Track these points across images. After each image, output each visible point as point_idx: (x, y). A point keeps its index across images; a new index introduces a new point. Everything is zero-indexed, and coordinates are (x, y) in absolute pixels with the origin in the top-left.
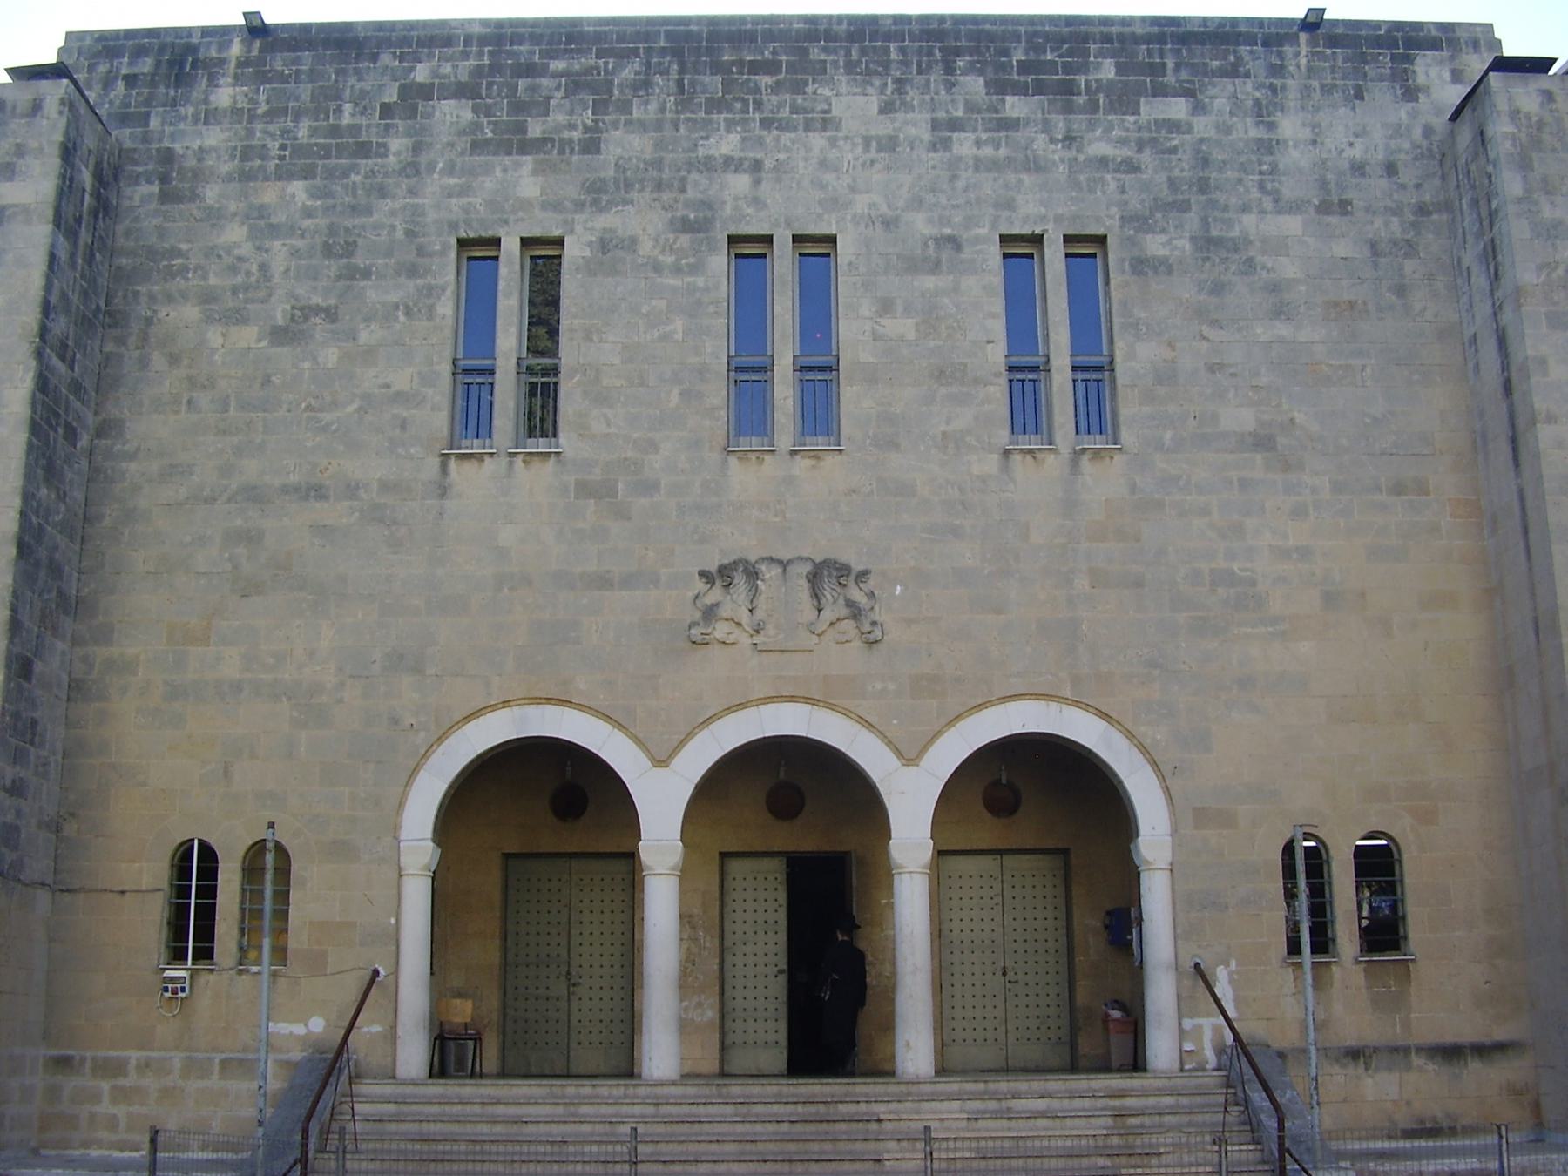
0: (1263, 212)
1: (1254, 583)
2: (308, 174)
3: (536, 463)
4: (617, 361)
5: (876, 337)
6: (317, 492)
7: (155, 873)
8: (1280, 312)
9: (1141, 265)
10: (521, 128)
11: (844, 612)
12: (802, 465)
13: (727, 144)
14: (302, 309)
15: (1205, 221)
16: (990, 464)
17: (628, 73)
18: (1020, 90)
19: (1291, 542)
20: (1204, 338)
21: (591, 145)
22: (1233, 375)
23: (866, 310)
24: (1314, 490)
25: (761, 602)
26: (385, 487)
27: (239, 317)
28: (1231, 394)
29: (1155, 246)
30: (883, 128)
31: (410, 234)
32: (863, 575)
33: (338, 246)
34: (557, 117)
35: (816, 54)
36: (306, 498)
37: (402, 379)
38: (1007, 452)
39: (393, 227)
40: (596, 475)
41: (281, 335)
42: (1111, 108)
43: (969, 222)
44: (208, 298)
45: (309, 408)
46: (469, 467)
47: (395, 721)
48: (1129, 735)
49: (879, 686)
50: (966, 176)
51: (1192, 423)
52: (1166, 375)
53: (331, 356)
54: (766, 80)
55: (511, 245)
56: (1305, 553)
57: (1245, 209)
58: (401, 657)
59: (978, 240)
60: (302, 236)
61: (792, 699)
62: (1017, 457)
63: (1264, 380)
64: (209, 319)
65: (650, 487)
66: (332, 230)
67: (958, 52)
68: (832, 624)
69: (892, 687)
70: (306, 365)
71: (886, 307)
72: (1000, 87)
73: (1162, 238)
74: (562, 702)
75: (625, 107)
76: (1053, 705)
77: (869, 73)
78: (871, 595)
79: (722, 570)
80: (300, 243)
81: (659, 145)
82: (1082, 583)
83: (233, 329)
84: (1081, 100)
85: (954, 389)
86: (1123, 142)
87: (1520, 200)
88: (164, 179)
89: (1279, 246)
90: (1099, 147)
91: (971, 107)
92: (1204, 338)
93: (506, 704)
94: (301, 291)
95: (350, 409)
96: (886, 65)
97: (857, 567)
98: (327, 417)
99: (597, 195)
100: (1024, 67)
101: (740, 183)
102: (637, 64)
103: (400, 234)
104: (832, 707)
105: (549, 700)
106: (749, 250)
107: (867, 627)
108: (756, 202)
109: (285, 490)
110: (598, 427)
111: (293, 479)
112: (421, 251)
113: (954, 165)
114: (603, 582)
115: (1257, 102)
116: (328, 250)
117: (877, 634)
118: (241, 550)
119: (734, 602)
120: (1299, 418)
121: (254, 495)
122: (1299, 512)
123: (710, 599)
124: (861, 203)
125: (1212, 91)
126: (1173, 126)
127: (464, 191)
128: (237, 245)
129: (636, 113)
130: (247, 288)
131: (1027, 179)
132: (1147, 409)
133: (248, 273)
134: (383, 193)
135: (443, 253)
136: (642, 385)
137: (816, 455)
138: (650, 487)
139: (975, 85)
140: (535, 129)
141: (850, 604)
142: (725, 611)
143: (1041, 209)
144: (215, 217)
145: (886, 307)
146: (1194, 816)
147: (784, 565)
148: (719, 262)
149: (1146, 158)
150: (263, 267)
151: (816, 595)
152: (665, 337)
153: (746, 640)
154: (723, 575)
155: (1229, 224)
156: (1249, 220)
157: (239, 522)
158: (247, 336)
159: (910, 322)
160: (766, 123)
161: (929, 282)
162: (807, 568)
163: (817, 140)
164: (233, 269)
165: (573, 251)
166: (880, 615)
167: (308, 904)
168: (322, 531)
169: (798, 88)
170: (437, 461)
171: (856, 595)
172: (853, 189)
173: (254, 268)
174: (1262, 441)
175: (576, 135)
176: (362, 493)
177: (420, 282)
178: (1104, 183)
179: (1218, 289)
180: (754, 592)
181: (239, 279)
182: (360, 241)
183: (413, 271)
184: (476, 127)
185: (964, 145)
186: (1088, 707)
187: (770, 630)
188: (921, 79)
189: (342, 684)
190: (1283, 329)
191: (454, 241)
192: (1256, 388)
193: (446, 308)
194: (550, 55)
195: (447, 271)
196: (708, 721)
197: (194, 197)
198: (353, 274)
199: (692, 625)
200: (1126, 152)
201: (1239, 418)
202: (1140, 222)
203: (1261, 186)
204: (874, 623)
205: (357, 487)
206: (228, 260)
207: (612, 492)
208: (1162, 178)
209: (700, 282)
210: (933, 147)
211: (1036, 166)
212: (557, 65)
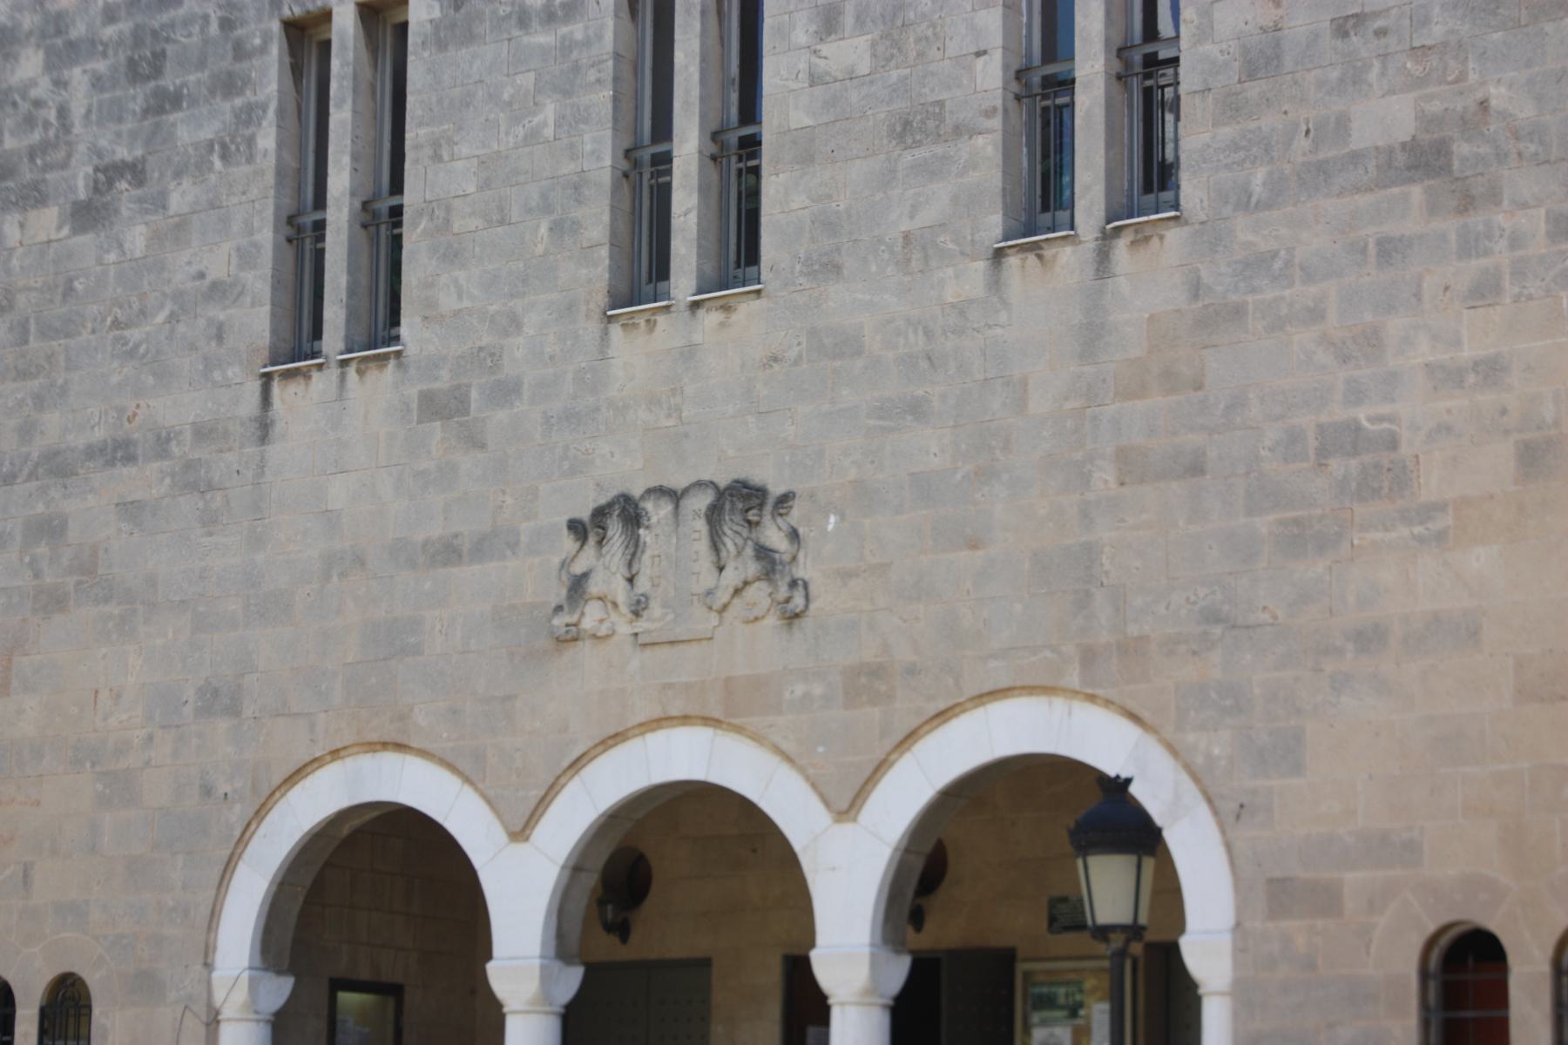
1: (1393, 443)
3: (373, 374)
4: (471, 189)
5: (815, 80)
6: (119, 452)
11: (753, 568)
14: (105, 170)
19: (1467, 353)
22: (1381, 33)
23: (801, 37)
24: (1515, 242)
25: (646, 565)
26: (203, 433)
27: (35, 197)
28: (1373, 75)
31: (227, 24)
32: (785, 500)
33: (144, 62)
36: (111, 463)
37: (219, 264)
38: (999, 254)
39: (206, 18)
40: (443, 381)
41: (87, 215)
45: (116, 324)
46: (294, 387)
47: (207, 791)
48: (1173, 750)
49: (800, 689)
51: (1302, 143)
53: (137, 238)
56: (1491, 370)
58: (216, 692)
60: (104, 55)
61: (685, 720)
62: (1013, 261)
63: (1437, 31)
65: (506, 392)
66: (137, 37)
68: (737, 592)
69: (818, 689)
70: (112, 257)
71: (829, 24)
74: (400, 747)
76: (1059, 703)
78: (794, 535)
79: (600, 514)
80: (101, 66)
82: (1105, 476)
83: (32, 214)
85: (922, 153)
93: (335, 754)
94: (103, 143)
95: (161, 318)
97: (776, 490)
98: (134, 334)
103: (214, 28)
104: (739, 730)
105: (385, 745)
107: (783, 591)
109: (91, 452)
110: (447, 302)
111: (99, 434)
112: (240, 52)
114: (448, 552)
116: (134, 72)
117: (798, 601)
118: (42, 550)
119: (605, 566)
120: (1498, 95)
121: (57, 466)
122: (1484, 292)
123: (578, 568)
128: (33, 83)
130: (45, 147)
132: (1227, 132)
133: (47, 125)
135: (263, 50)
136: (502, 222)
137: (727, 309)
138: (506, 392)
141: (764, 553)
142: (594, 587)
145: (829, 24)
150: (63, 112)
151: (716, 545)
152: (533, 137)
153: (624, 629)
157: (40, 508)
158: (47, 221)
159: (863, 42)
162: (701, 502)
164: (30, 121)
168: (130, 510)
170: (255, 386)
171: (773, 536)
173: (52, 116)
174: (1425, 159)
176: (174, 448)
177: (238, 102)
180: (634, 548)
181: (36, 136)
182: (170, 49)
183: (229, 85)
186: (1108, 703)
187: (655, 609)
189: (150, 738)
191: (276, 26)
193: (267, 140)
195: (269, 74)
196: (577, 765)
199: (559, 609)
201: (1386, 117)
204: (793, 584)
205: (168, 440)
206: (24, 107)
207: (462, 405)
209: (577, 30)
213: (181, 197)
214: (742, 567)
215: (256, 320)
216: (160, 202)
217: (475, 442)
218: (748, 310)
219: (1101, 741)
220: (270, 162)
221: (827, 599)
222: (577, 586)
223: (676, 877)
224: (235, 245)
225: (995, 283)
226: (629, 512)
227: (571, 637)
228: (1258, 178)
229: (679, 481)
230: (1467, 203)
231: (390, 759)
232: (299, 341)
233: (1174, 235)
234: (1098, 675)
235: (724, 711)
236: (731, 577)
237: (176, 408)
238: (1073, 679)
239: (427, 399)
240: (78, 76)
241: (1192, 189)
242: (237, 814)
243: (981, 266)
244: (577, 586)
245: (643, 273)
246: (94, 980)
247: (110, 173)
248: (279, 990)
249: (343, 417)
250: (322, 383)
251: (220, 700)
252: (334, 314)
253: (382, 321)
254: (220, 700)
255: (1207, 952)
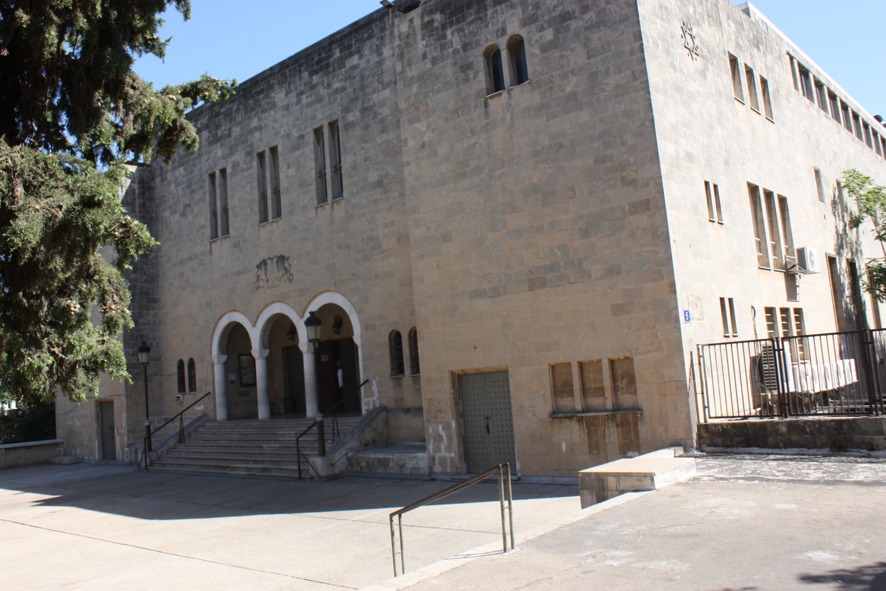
0: (379, 91)
1: (378, 239)
2: (182, 165)
6: (190, 259)
7: (174, 370)
8: (384, 130)
9: (349, 126)
10: (217, 134)
12: (275, 224)
13: (254, 123)
15: (363, 103)
16: (312, 213)
17: (235, 107)
18: (315, 72)
20: (363, 149)
21: (229, 135)
23: (285, 169)
25: (268, 272)
26: (203, 254)
27: (175, 212)
29: (350, 117)
30: (285, 103)
32: (288, 258)
33: (189, 186)
34: (223, 128)
35: (272, 82)
37: (202, 222)
42: (339, 69)
43: (306, 127)
44: (170, 208)
50: (305, 110)
52: (354, 167)
54: (261, 96)
55: (218, 173)
57: (374, 92)
59: (308, 133)
61: (277, 301)
64: (171, 214)
65: (245, 241)
67: (301, 65)
71: (289, 166)
72: (312, 74)
73: (352, 114)
74: (235, 311)
75: (235, 120)
77: (283, 83)
81: (242, 129)
84: (331, 69)
86: (341, 80)
87: (401, 73)
88: (161, 175)
89: (382, 104)
90: (336, 85)
91: (305, 85)
92: (363, 149)
93: (226, 313)
96: (286, 78)
99: (232, 150)
100: (318, 63)
101: (257, 134)
102: (236, 104)
106: (261, 156)
108: (261, 140)
112: (203, 181)
113: (301, 109)
114: (239, 273)
115: (377, 47)
120: (390, 170)
121: (182, 263)
122: (390, 208)
124: (282, 133)
125: (365, 48)
126: (354, 67)
127: (208, 159)
129: (238, 120)
131: (319, 105)
134: (195, 165)
138: (245, 241)
139: (305, 75)
140: (219, 134)
141: (285, 269)
143: (322, 118)
144: (170, 183)
145: (289, 166)
146: (367, 327)
147: (271, 259)
148: (255, 163)
149: (348, 84)
154: (258, 267)
155: (369, 100)
156: (375, 96)
158: (177, 216)
160: (262, 112)
161: (298, 153)
162: (275, 260)
163: (272, 113)
165: (229, 171)
166: (292, 271)
167: (199, 375)
168: (193, 270)
169: (267, 96)
170: (209, 244)
171: (287, 265)
172: (281, 127)
174: (379, 184)
175: (226, 132)
178: (336, 98)
179: (366, 128)
180: (266, 270)
183: (202, 187)
184: (209, 137)
185: (304, 101)
188: (293, 80)
190: (385, 137)
192: (377, 163)
193: (208, 197)
194: (221, 108)
195: (207, 185)
197: (166, 178)
198: (193, 192)
200: (342, 84)
201: (373, 176)
202: (346, 110)
203: (379, 82)
208: (351, 90)
209: (251, 171)
210: (297, 104)
211: (320, 100)
212: (222, 110)
213: (196, 210)
214: (283, 272)
215: (208, 232)
216: (193, 211)
217: (242, 251)
218: (280, 222)
219: (339, 300)
220: (208, 202)
221: (295, 276)
222: (258, 277)
223: (280, 330)
224: (204, 219)
225: (317, 213)
226: (264, 263)
227: (258, 287)
228: (355, 189)
229: (272, 256)
230: (386, 192)
231: (234, 313)
232: (214, 236)
233: (343, 202)
234: (337, 287)
235: (282, 299)
236: (281, 274)
237: (198, 250)
238: (333, 288)
239: (234, 244)
240: (180, 188)
241: (345, 193)
242: (213, 325)
243: (314, 211)
244: (258, 277)
245: (264, 219)
246: (195, 358)
247: (187, 206)
248: (224, 358)
249: (222, 247)
250: (219, 242)
251: (209, 305)
252: (219, 229)
253: (226, 231)
254: (209, 305)
255: (357, 339)
